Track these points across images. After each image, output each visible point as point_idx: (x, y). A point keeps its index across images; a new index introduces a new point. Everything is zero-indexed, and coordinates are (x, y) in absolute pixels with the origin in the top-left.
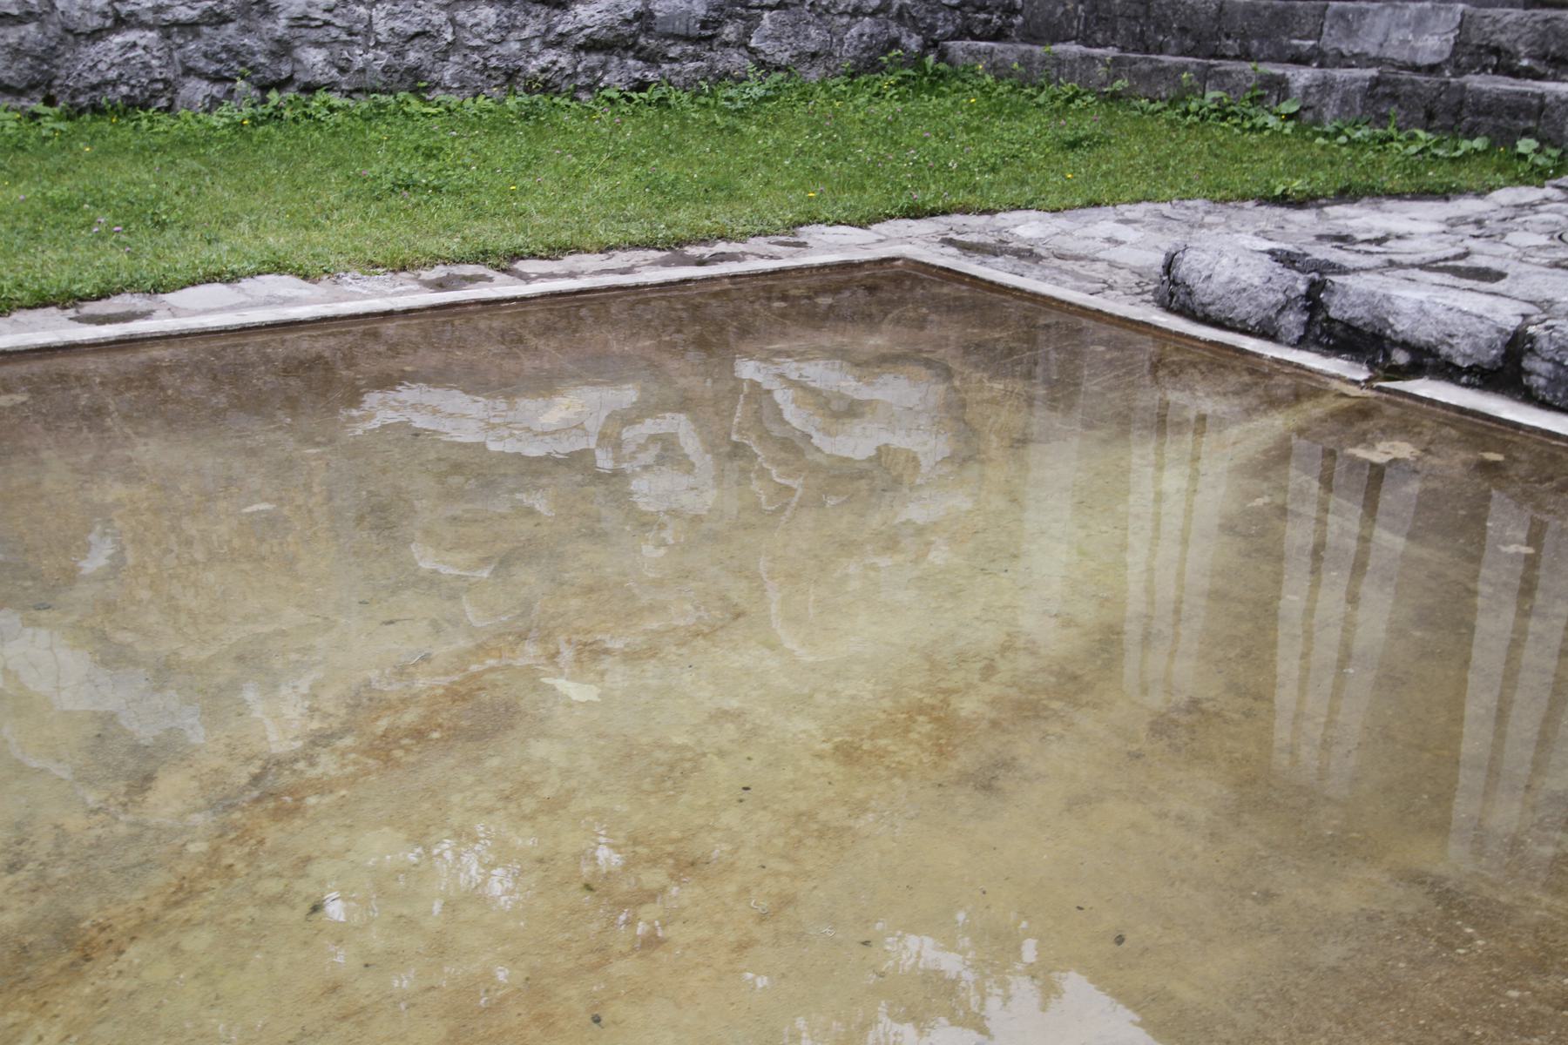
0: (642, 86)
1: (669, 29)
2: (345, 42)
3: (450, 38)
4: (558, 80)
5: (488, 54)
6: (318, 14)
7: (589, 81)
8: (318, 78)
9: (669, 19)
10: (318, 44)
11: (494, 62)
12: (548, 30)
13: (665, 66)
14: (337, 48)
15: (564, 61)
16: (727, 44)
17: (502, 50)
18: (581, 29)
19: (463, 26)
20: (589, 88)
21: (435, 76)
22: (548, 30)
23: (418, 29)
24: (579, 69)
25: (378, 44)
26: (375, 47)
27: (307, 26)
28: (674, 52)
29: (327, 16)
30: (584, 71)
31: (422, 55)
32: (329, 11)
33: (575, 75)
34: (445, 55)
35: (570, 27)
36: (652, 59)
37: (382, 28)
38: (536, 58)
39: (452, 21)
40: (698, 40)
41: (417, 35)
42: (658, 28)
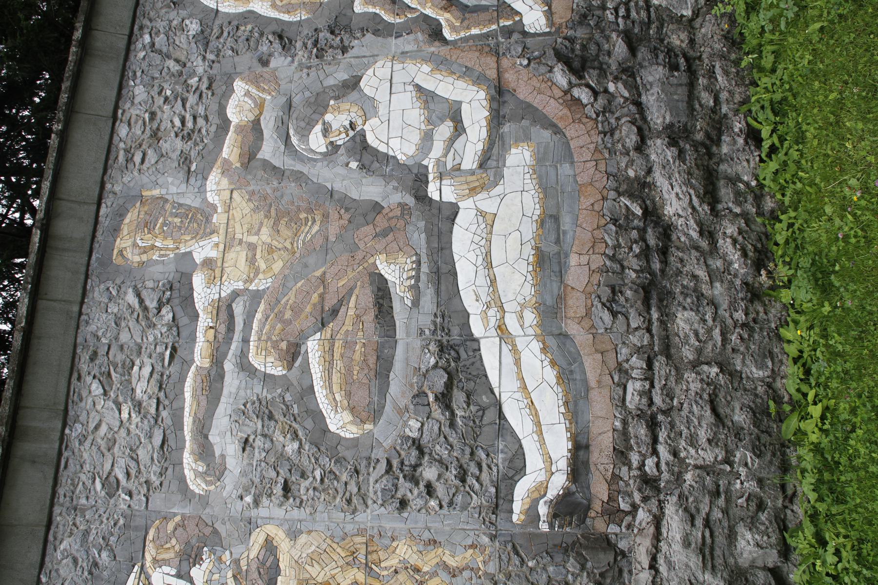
0: (753, 136)
1: (682, 106)
2: (728, 501)
3: (715, 370)
4: (753, 236)
5: (729, 321)
6: (697, 534)
7: (750, 198)
8: (773, 540)
9: (672, 108)
10: (732, 536)
11: (740, 316)
12: (697, 248)
13: (724, 109)
14: (735, 511)
15: (731, 230)
16: (692, 41)
17: (724, 304)
18: (693, 208)
19: (699, 351)
20: (758, 199)
21: (760, 390)
22: (697, 248)
23: (708, 408)
24: (738, 210)
25: (728, 461)
26: (731, 464)
27: (712, 549)
28: (707, 99)
29: (699, 522)
30: (738, 203)
31: (737, 405)
32: (692, 518)
33: (745, 215)
34: (734, 375)
35: (692, 222)
36: (718, 126)
37: (708, 456)
38: (730, 263)
39: (695, 365)
40: (691, 72)
41: (714, 410)
42: (684, 119)
